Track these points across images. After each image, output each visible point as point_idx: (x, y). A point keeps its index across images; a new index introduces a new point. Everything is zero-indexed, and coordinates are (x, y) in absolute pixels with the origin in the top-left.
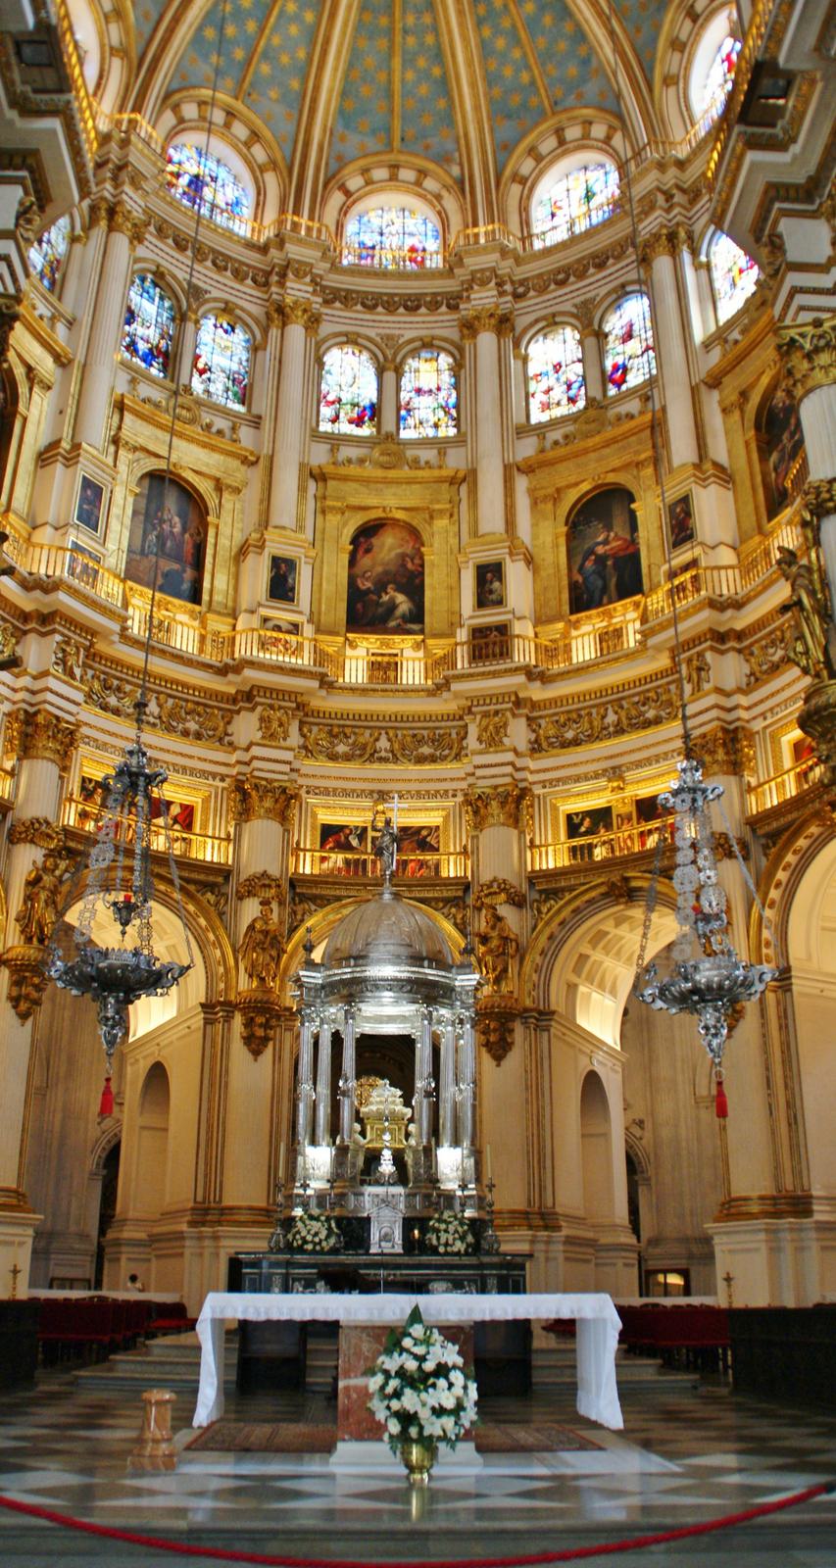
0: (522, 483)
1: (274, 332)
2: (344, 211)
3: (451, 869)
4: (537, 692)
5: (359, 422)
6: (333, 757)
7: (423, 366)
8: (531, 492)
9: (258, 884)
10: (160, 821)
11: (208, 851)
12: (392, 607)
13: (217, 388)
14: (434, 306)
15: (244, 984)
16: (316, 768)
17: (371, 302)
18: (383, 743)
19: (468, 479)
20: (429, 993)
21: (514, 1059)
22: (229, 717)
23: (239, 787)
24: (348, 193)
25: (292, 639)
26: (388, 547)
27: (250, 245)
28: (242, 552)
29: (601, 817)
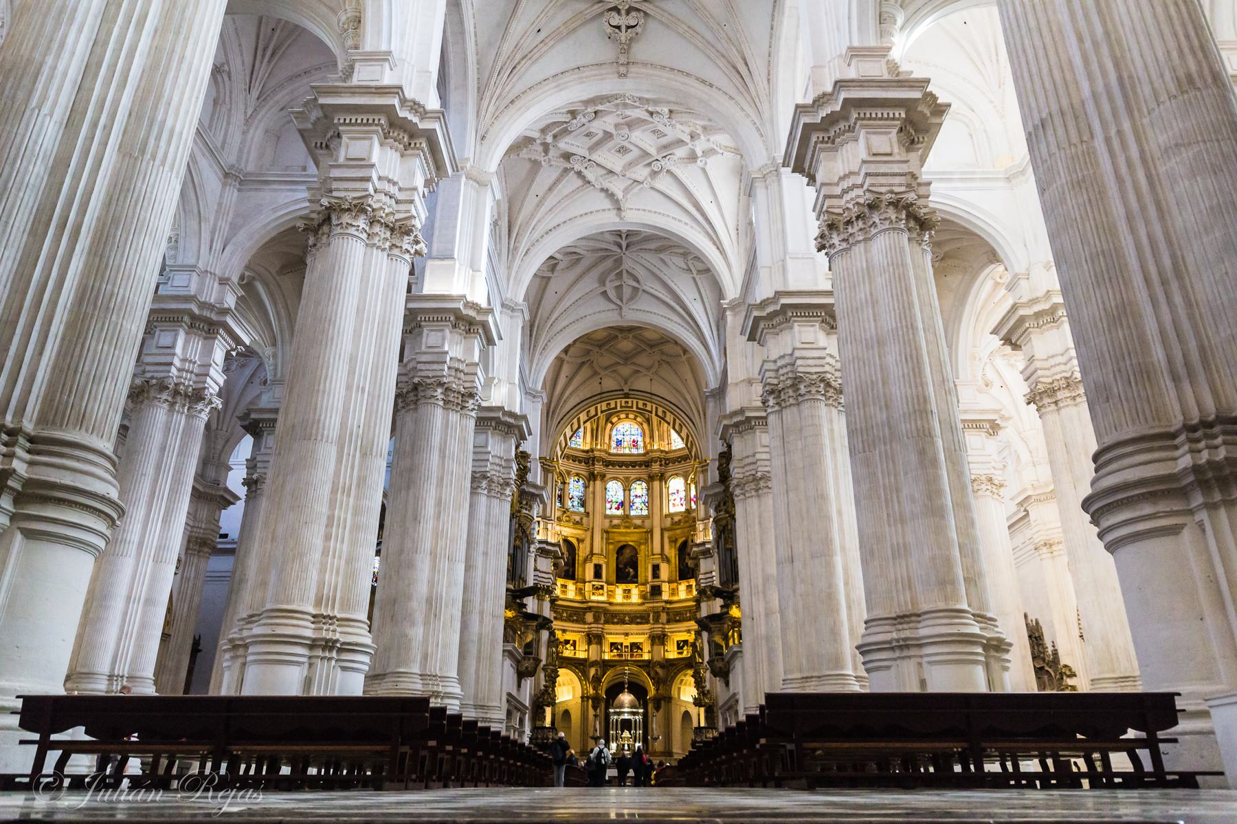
0: (666, 535)
1: (591, 483)
2: (611, 430)
3: (646, 657)
4: (668, 606)
5: (618, 508)
6: (613, 623)
7: (638, 487)
8: (669, 538)
9: (594, 664)
10: (568, 646)
11: (581, 655)
12: (629, 572)
13: (575, 503)
14: (640, 465)
15: (592, 692)
16: (610, 627)
17: (621, 464)
18: (627, 618)
19: (651, 532)
20: (634, 714)
21: (661, 711)
22: (584, 614)
23: (588, 635)
24: (612, 424)
25: (601, 591)
26: (627, 553)
27: (583, 451)
28: (585, 561)
29: (686, 642)
